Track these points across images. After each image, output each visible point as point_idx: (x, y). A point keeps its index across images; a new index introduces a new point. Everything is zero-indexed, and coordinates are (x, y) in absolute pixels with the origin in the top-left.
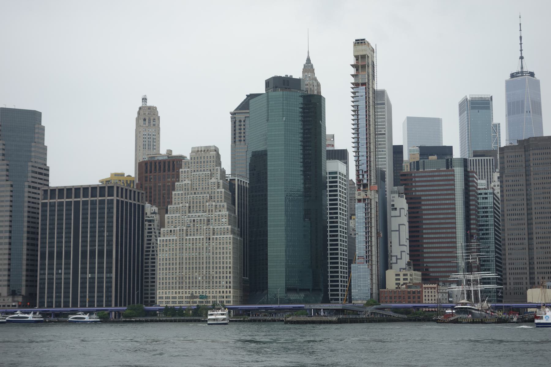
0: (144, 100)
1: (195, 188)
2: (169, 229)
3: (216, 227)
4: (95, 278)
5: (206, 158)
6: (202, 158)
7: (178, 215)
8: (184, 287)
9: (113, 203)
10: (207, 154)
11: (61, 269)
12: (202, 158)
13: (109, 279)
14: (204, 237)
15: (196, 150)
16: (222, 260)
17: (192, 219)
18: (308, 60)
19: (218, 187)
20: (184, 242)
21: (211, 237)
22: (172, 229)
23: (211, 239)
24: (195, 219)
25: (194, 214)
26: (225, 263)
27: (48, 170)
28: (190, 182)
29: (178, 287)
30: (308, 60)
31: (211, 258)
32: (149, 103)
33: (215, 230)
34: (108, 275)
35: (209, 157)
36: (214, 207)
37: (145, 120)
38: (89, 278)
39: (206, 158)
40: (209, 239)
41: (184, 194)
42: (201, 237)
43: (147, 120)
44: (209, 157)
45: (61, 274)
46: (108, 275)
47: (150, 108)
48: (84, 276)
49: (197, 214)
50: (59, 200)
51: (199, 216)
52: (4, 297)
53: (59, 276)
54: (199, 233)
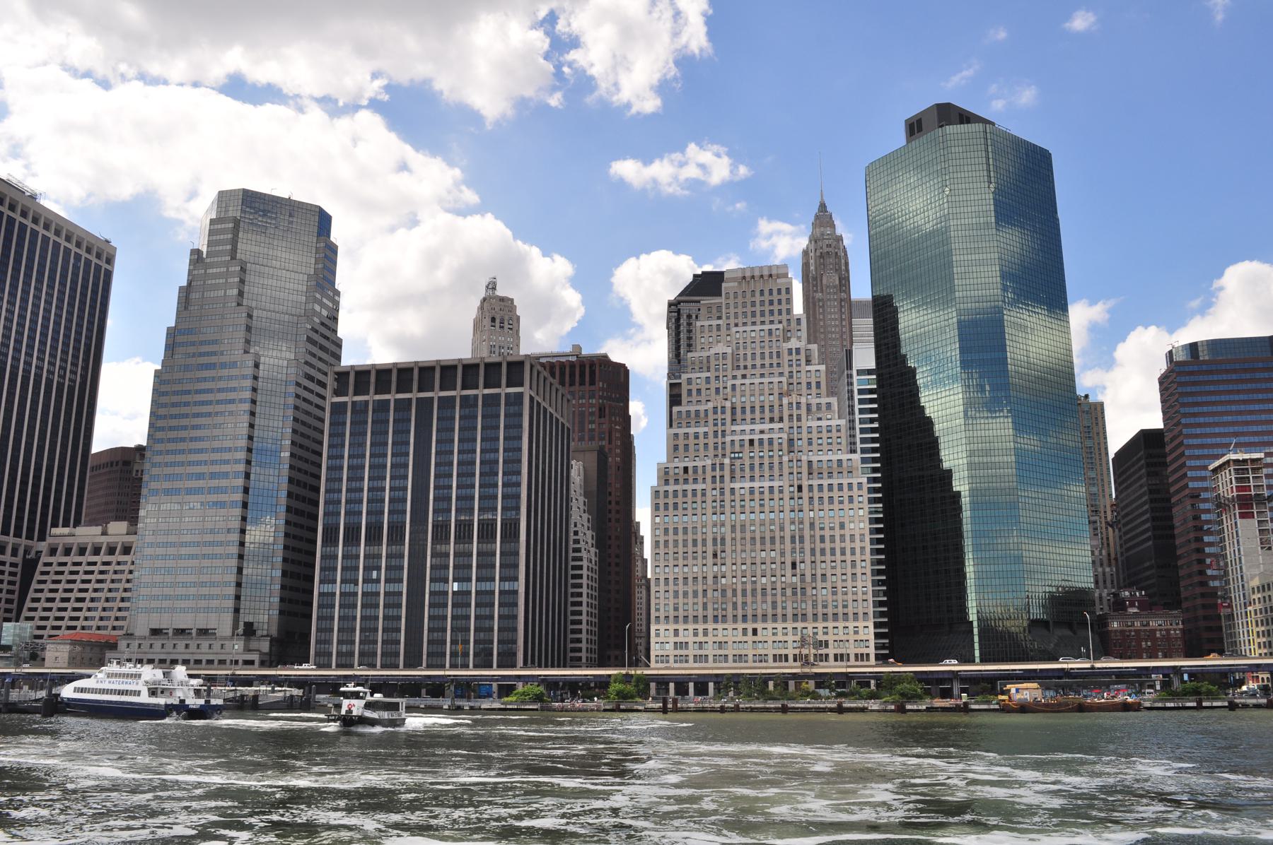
0: (492, 286)
1: (742, 364)
2: (682, 465)
3: (815, 459)
4: (470, 593)
5: (767, 293)
6: (758, 294)
7: (701, 430)
8: (730, 617)
9: (521, 403)
10: (771, 285)
11: (379, 569)
12: (758, 294)
13: (509, 598)
14: (785, 483)
15: (740, 275)
16: (838, 545)
17: (747, 438)
18: (823, 207)
19: (808, 362)
20: (727, 496)
21: (805, 484)
22: (690, 465)
23: (805, 489)
24: (756, 437)
25: (748, 428)
26: (848, 552)
27: (340, 346)
28: (729, 350)
29: (710, 618)
30: (823, 207)
31: (807, 538)
32: (500, 292)
33: (815, 466)
34: (507, 586)
35: (775, 292)
36: (804, 407)
37: (493, 320)
38: (454, 593)
39: (767, 293)
40: (800, 488)
41: (713, 380)
42: (776, 484)
43: (498, 321)
44: (775, 292)
45: (378, 581)
46: (507, 586)
47: (502, 299)
48: (439, 587)
49: (758, 427)
50: (378, 397)
51: (762, 432)
52: (225, 638)
53: (371, 588)
54: (767, 475)
